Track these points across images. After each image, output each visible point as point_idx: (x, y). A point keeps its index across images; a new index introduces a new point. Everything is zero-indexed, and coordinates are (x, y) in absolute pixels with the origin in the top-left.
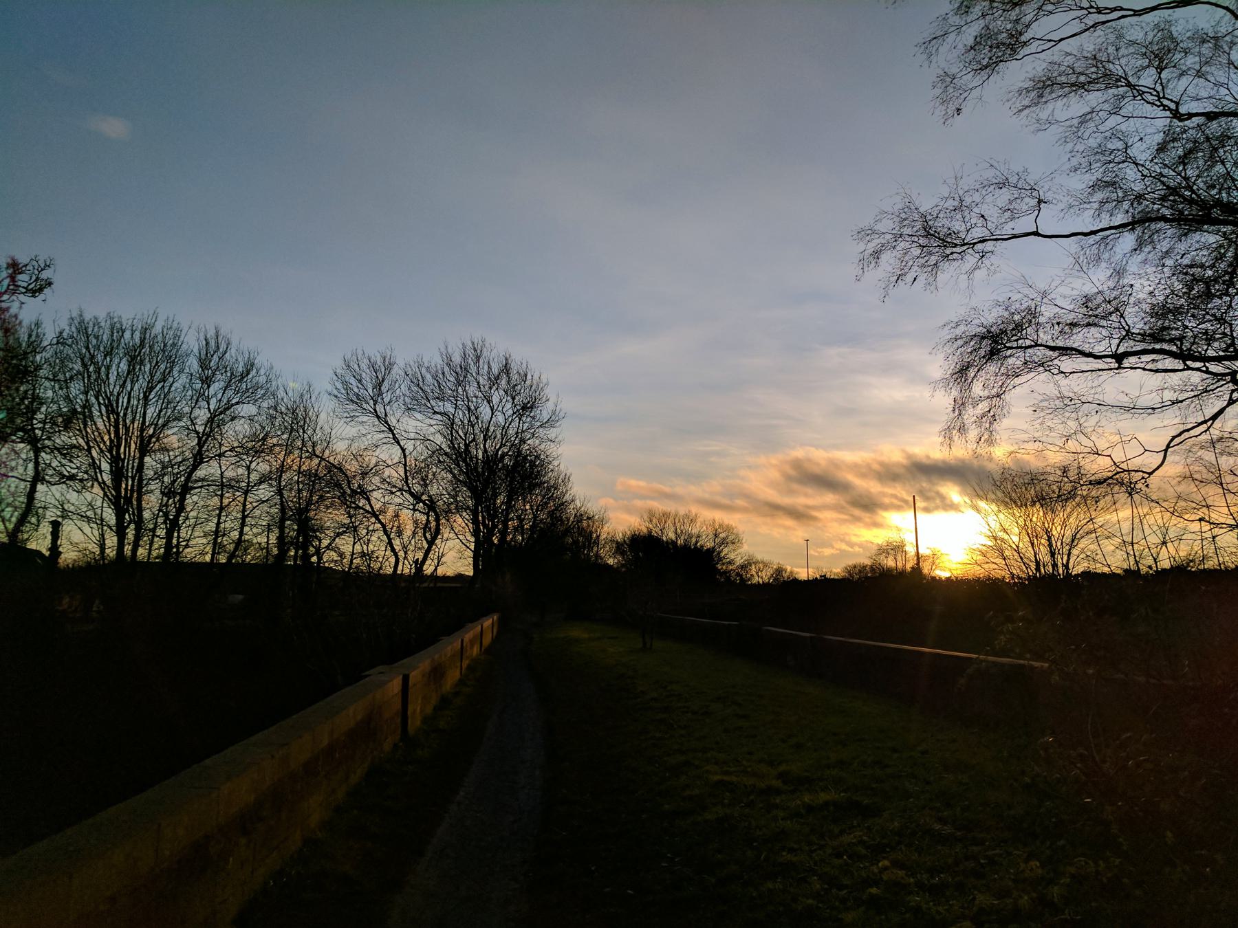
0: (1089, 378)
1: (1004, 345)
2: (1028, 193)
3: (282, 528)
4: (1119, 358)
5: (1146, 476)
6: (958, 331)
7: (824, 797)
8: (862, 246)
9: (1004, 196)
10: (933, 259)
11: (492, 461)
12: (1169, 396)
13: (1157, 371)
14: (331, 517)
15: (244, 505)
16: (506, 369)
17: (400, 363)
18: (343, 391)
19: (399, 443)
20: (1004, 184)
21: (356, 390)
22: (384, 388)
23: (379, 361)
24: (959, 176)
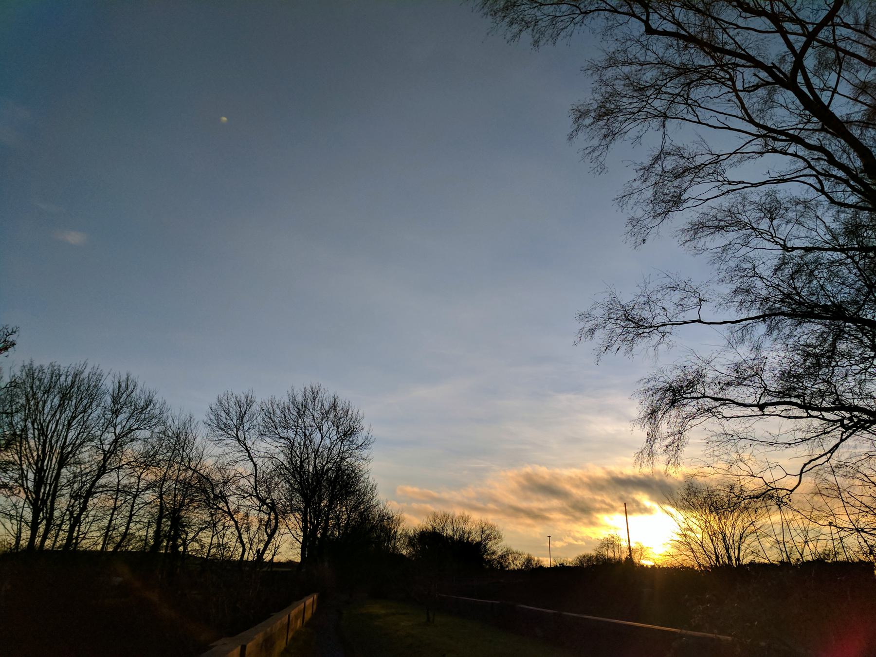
0: (742, 421)
1: (682, 396)
3: (159, 524)
4: (762, 407)
5: (789, 492)
6: (650, 385)
8: (581, 325)
9: (677, 296)
10: (631, 336)
11: (319, 474)
12: (800, 435)
13: (789, 418)
14: (197, 516)
15: (132, 506)
16: (334, 406)
17: (258, 400)
18: (216, 422)
19: (252, 460)
20: (676, 288)
21: (225, 421)
22: (245, 419)
23: (243, 400)
24: (648, 281)
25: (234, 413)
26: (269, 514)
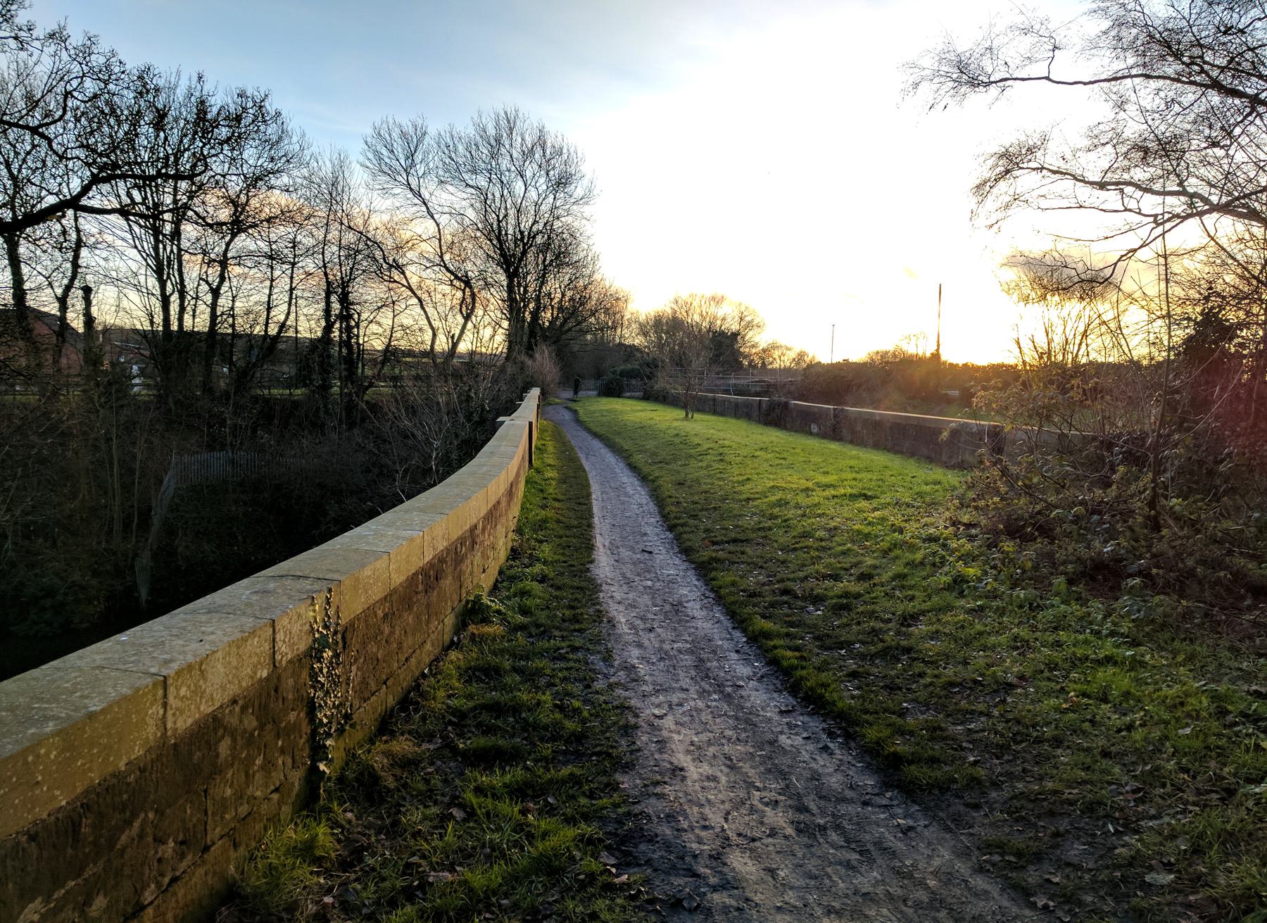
2: (1046, 40)
3: (328, 303)
7: (842, 491)
9: (1029, 40)
10: (964, 88)
11: (526, 240)
14: (367, 292)
15: (292, 278)
16: (541, 142)
17: (432, 131)
18: (375, 162)
19: (432, 217)
25: (400, 150)
26: (464, 291)
